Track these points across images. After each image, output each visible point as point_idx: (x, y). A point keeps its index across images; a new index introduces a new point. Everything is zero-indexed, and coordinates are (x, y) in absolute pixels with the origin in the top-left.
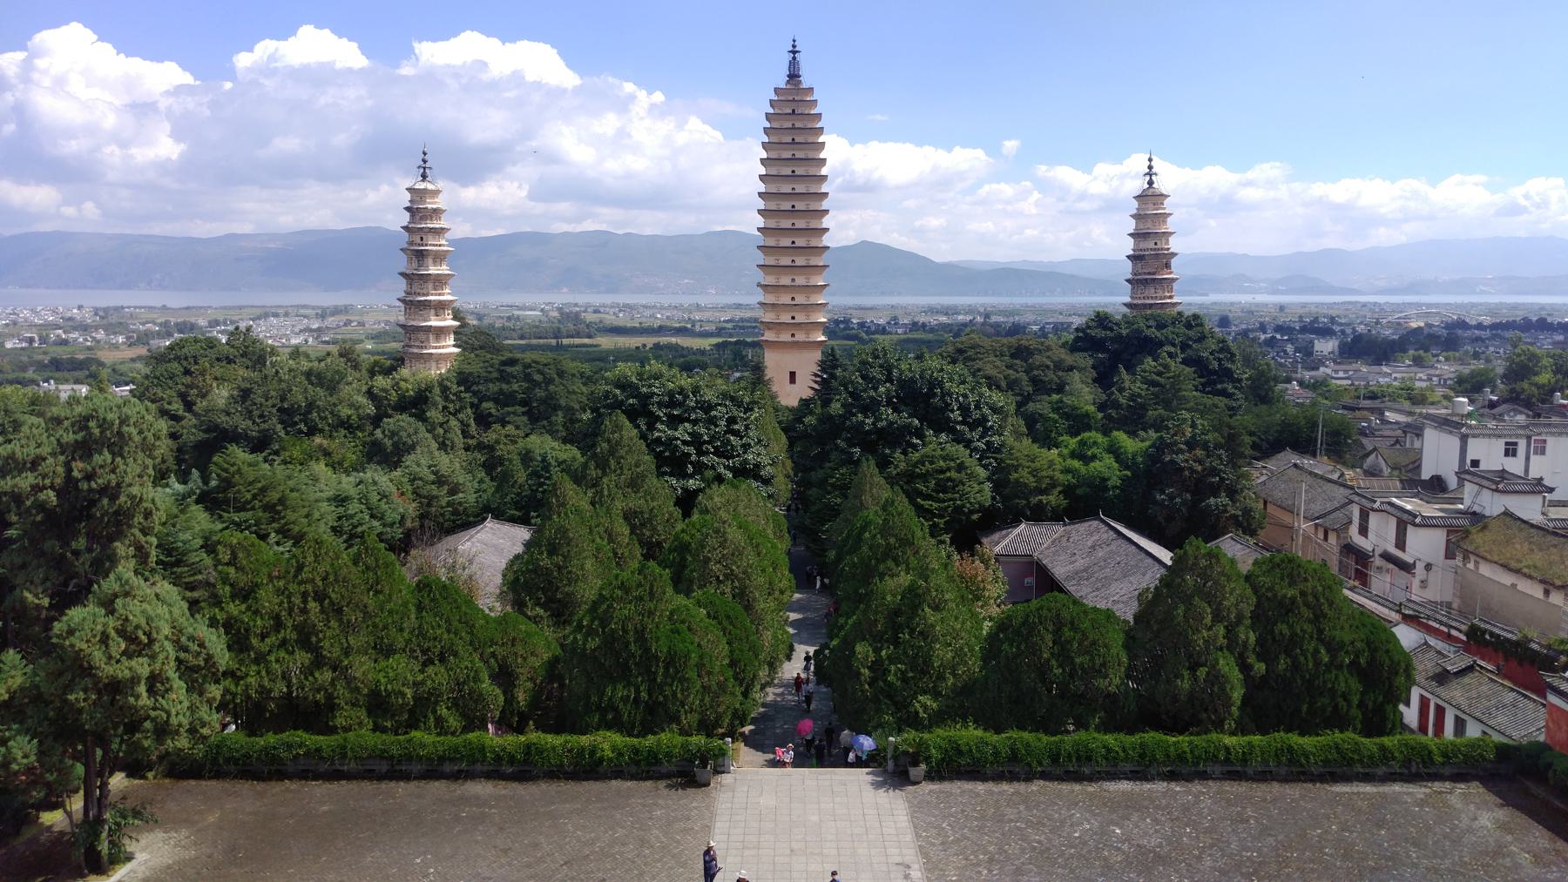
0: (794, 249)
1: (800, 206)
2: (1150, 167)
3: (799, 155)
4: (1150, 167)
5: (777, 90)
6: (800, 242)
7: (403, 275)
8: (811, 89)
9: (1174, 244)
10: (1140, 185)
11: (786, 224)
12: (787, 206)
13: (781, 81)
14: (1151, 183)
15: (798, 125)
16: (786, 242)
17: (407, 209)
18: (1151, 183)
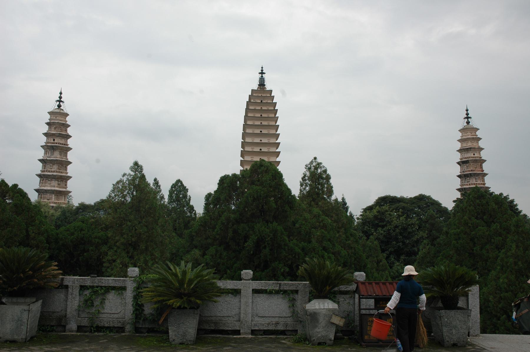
2: (467, 114)
5: (253, 91)
7: (40, 160)
8: (271, 91)
9: (483, 155)
10: (463, 123)
12: (257, 149)
13: (256, 87)
14: (468, 123)
17: (48, 124)
18: (468, 123)
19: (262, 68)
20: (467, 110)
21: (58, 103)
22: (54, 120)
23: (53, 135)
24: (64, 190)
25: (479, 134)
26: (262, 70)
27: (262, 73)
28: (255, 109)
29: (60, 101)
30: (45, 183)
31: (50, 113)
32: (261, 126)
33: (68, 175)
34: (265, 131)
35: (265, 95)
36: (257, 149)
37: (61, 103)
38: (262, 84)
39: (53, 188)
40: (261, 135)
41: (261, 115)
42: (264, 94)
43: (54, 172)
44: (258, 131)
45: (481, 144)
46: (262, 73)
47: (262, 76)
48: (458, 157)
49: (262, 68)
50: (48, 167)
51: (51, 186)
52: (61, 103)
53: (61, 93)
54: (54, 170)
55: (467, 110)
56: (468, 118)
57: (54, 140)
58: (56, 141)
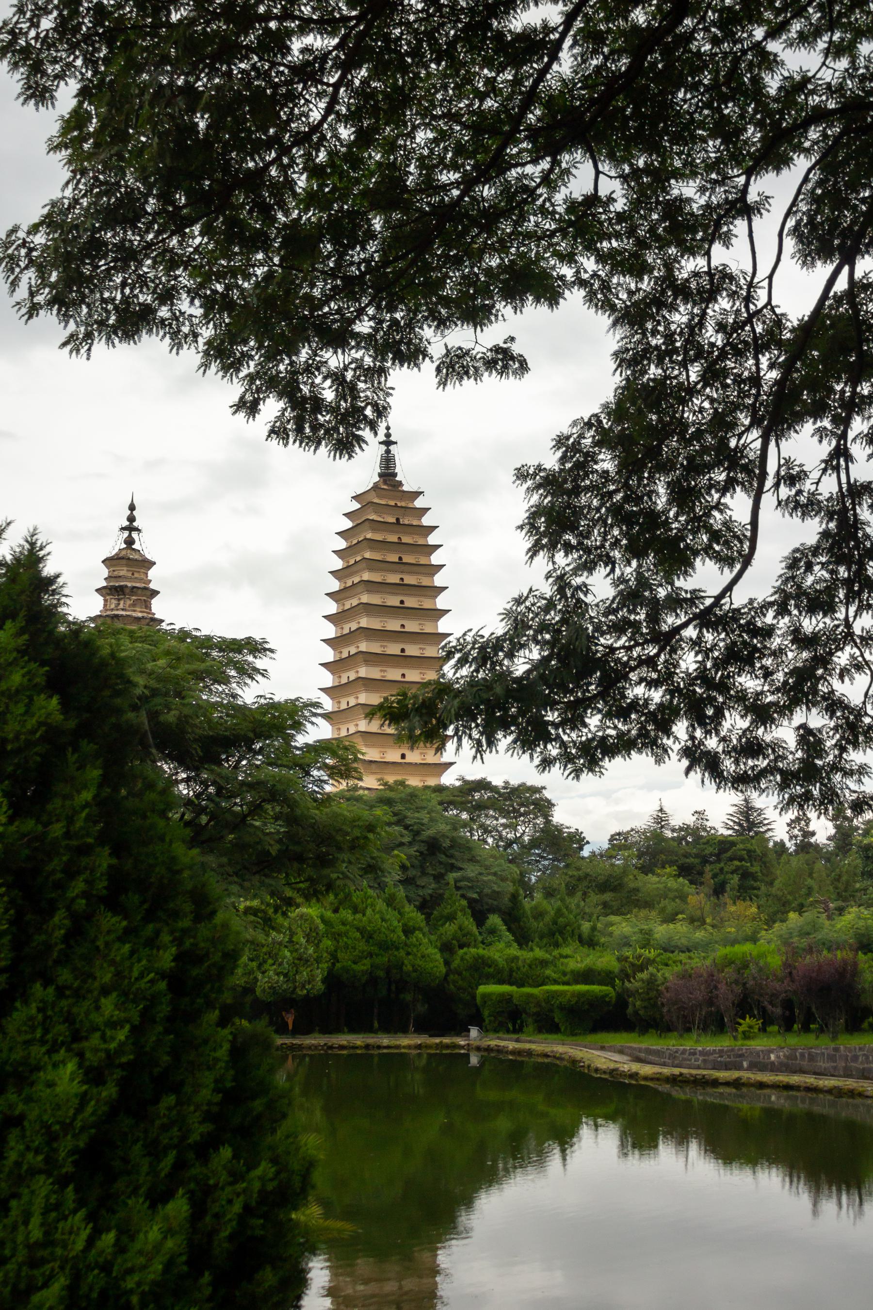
3: (410, 580)
12: (394, 649)
15: (405, 539)
29: (131, 528)
32: (401, 586)
34: (411, 602)
35: (403, 504)
36: (394, 649)
37: (135, 535)
40: (402, 610)
41: (400, 559)
42: (401, 500)
47: (388, 452)
52: (135, 535)
53: (132, 508)
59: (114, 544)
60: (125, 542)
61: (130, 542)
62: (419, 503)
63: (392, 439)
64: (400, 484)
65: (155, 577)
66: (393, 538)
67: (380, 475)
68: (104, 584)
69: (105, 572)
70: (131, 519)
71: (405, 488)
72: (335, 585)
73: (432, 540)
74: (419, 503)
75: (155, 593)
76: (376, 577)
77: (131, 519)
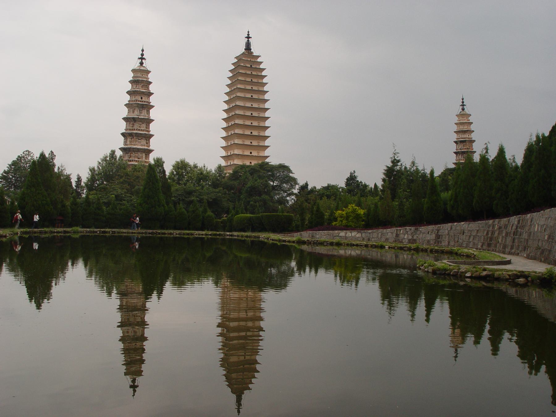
0: (251, 137)
1: (255, 114)
2: (463, 102)
3: (255, 88)
4: (463, 102)
6: (255, 133)
11: (248, 123)
12: (248, 113)
14: (463, 109)
15: (254, 73)
16: (248, 132)
18: (463, 109)
19: (248, 32)
20: (463, 99)
21: (140, 60)
22: (141, 77)
23: (143, 93)
24: (146, 148)
25: (471, 119)
26: (248, 35)
27: (248, 37)
28: (246, 74)
29: (142, 58)
30: (136, 141)
31: (134, 71)
32: (252, 91)
33: (151, 133)
37: (143, 61)
38: (248, 47)
39: (143, 147)
40: (252, 99)
42: (253, 58)
43: (142, 130)
44: (249, 96)
45: (472, 127)
46: (248, 37)
47: (248, 41)
48: (455, 137)
49: (248, 32)
50: (136, 126)
51: (142, 145)
52: (143, 61)
53: (143, 51)
54: (139, 129)
55: (463, 99)
56: (463, 105)
57: (142, 98)
58: (143, 100)
59: (136, 64)
60: (140, 63)
61: (142, 64)
62: (259, 60)
63: (250, 36)
64: (252, 53)
65: (151, 77)
66: (249, 72)
67: (245, 49)
68: (132, 79)
69: (132, 75)
70: (142, 55)
71: (254, 54)
72: (228, 90)
73: (263, 73)
74: (259, 60)
75: (150, 83)
76: (242, 86)
77: (142, 55)
